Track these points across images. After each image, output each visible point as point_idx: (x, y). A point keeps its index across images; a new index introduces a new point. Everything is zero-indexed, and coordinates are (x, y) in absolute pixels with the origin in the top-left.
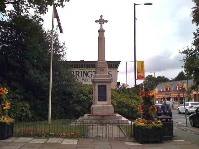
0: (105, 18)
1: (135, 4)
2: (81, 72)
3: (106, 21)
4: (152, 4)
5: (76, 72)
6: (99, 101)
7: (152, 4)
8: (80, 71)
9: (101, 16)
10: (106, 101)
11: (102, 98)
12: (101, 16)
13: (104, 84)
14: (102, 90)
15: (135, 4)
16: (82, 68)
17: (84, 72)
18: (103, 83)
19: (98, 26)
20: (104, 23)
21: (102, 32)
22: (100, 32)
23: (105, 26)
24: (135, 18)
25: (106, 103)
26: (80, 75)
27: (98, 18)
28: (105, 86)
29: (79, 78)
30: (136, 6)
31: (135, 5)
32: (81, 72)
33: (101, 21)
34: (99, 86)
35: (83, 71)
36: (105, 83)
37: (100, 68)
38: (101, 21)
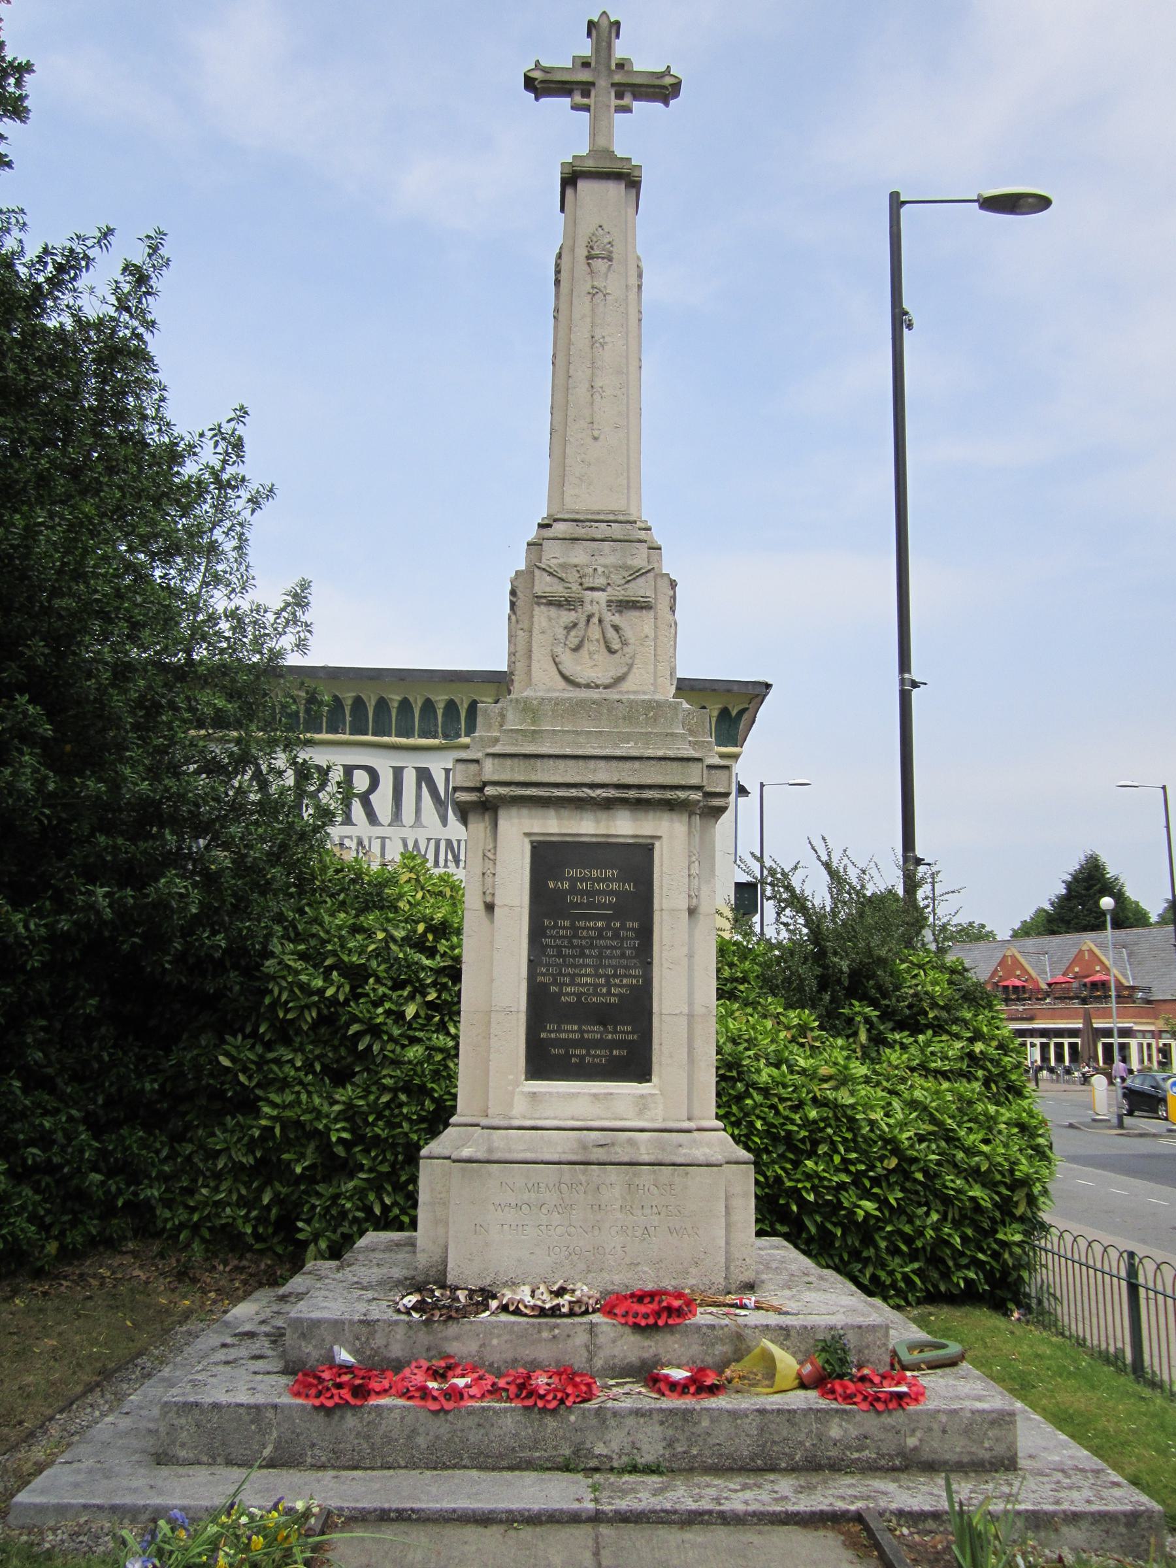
0: (640, 53)
1: (894, 196)
2: (398, 773)
3: (662, 90)
4: (1043, 203)
5: (349, 770)
6: (544, 1061)
7: (1043, 203)
8: (384, 764)
9: (603, 31)
10: (643, 1073)
11: (591, 1024)
12: (603, 31)
13: (624, 826)
14: (593, 918)
15: (894, 196)
16: (408, 733)
17: (424, 775)
18: (607, 805)
19: (564, 130)
20: (637, 105)
21: (614, 190)
22: (582, 185)
23: (636, 132)
24: (900, 320)
25: (642, 1104)
26: (382, 800)
27: (566, 50)
28: (637, 860)
29: (378, 831)
30: (904, 210)
31: (896, 203)
32: (398, 773)
33: (600, 79)
34: (547, 858)
35: (410, 764)
36: (640, 805)
37: (567, 617)
38: (600, 79)
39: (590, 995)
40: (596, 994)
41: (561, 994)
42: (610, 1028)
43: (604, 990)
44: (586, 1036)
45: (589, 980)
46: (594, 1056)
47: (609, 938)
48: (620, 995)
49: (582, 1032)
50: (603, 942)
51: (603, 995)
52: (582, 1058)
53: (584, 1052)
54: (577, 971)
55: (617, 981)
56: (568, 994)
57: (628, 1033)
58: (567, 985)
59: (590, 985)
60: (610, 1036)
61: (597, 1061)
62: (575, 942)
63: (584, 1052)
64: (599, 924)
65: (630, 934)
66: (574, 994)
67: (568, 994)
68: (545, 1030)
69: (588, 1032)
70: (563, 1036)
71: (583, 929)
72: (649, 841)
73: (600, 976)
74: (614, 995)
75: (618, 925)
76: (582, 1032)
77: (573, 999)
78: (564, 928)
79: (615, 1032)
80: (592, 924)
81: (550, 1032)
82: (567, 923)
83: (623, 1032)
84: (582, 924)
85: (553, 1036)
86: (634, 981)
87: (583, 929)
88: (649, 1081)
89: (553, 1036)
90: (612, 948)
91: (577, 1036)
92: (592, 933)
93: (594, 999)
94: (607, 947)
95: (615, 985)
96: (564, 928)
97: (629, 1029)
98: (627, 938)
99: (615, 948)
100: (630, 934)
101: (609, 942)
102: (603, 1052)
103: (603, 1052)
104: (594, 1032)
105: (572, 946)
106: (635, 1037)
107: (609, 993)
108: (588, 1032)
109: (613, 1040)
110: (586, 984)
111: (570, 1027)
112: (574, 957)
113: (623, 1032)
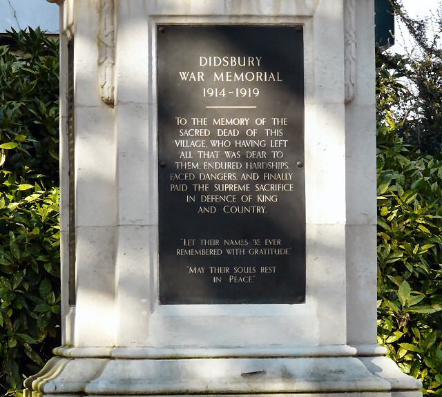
39: (232, 204)
40: (239, 203)
41: (198, 203)
42: (256, 242)
43: (249, 199)
44: (229, 252)
45: (231, 187)
46: (238, 275)
47: (252, 138)
48: (266, 204)
49: (224, 247)
50: (245, 143)
51: (247, 205)
52: (225, 276)
53: (227, 270)
54: (217, 177)
55: (263, 188)
56: (207, 205)
57: (277, 247)
58: (206, 194)
59: (232, 193)
60: (256, 252)
61: (242, 280)
62: (213, 143)
63: (227, 270)
64: (242, 121)
65: (277, 132)
66: (214, 204)
67: (207, 205)
68: (181, 246)
69: (231, 247)
70: (203, 252)
71: (222, 128)
72: (297, 21)
73: (242, 183)
74: (260, 204)
75: (263, 122)
76: (224, 247)
77: (211, 210)
78: (199, 127)
79: (262, 246)
80: (232, 122)
81: (187, 248)
82: (204, 121)
83: (272, 246)
84: (220, 122)
85: (190, 252)
86: (284, 187)
87: (222, 128)
88: (302, 301)
89: (190, 252)
90: (257, 149)
91: (219, 252)
92: (232, 133)
93: (237, 209)
94: (250, 149)
95: (261, 192)
96: (199, 127)
97: (279, 242)
98: (274, 137)
99: (261, 149)
100: (277, 132)
101: (253, 143)
102: (249, 270)
103: (249, 270)
104: (236, 247)
105: (211, 149)
106: (286, 252)
107: (254, 202)
108: (231, 247)
109: (260, 256)
110: (228, 192)
111: (210, 242)
112: (211, 160)
113: (272, 246)
